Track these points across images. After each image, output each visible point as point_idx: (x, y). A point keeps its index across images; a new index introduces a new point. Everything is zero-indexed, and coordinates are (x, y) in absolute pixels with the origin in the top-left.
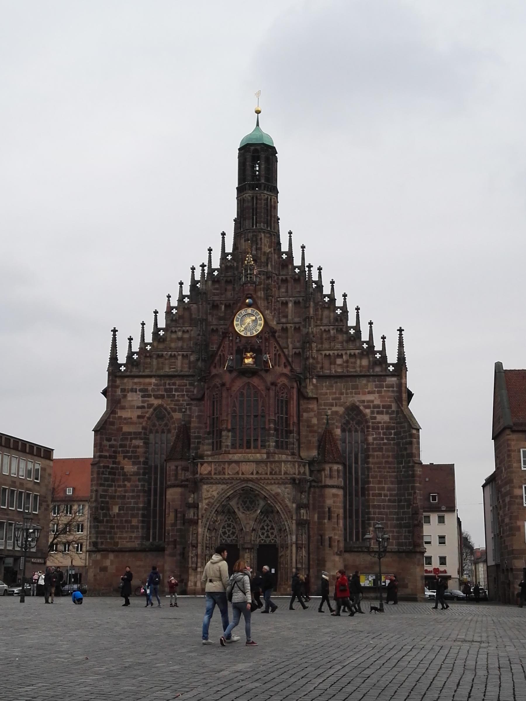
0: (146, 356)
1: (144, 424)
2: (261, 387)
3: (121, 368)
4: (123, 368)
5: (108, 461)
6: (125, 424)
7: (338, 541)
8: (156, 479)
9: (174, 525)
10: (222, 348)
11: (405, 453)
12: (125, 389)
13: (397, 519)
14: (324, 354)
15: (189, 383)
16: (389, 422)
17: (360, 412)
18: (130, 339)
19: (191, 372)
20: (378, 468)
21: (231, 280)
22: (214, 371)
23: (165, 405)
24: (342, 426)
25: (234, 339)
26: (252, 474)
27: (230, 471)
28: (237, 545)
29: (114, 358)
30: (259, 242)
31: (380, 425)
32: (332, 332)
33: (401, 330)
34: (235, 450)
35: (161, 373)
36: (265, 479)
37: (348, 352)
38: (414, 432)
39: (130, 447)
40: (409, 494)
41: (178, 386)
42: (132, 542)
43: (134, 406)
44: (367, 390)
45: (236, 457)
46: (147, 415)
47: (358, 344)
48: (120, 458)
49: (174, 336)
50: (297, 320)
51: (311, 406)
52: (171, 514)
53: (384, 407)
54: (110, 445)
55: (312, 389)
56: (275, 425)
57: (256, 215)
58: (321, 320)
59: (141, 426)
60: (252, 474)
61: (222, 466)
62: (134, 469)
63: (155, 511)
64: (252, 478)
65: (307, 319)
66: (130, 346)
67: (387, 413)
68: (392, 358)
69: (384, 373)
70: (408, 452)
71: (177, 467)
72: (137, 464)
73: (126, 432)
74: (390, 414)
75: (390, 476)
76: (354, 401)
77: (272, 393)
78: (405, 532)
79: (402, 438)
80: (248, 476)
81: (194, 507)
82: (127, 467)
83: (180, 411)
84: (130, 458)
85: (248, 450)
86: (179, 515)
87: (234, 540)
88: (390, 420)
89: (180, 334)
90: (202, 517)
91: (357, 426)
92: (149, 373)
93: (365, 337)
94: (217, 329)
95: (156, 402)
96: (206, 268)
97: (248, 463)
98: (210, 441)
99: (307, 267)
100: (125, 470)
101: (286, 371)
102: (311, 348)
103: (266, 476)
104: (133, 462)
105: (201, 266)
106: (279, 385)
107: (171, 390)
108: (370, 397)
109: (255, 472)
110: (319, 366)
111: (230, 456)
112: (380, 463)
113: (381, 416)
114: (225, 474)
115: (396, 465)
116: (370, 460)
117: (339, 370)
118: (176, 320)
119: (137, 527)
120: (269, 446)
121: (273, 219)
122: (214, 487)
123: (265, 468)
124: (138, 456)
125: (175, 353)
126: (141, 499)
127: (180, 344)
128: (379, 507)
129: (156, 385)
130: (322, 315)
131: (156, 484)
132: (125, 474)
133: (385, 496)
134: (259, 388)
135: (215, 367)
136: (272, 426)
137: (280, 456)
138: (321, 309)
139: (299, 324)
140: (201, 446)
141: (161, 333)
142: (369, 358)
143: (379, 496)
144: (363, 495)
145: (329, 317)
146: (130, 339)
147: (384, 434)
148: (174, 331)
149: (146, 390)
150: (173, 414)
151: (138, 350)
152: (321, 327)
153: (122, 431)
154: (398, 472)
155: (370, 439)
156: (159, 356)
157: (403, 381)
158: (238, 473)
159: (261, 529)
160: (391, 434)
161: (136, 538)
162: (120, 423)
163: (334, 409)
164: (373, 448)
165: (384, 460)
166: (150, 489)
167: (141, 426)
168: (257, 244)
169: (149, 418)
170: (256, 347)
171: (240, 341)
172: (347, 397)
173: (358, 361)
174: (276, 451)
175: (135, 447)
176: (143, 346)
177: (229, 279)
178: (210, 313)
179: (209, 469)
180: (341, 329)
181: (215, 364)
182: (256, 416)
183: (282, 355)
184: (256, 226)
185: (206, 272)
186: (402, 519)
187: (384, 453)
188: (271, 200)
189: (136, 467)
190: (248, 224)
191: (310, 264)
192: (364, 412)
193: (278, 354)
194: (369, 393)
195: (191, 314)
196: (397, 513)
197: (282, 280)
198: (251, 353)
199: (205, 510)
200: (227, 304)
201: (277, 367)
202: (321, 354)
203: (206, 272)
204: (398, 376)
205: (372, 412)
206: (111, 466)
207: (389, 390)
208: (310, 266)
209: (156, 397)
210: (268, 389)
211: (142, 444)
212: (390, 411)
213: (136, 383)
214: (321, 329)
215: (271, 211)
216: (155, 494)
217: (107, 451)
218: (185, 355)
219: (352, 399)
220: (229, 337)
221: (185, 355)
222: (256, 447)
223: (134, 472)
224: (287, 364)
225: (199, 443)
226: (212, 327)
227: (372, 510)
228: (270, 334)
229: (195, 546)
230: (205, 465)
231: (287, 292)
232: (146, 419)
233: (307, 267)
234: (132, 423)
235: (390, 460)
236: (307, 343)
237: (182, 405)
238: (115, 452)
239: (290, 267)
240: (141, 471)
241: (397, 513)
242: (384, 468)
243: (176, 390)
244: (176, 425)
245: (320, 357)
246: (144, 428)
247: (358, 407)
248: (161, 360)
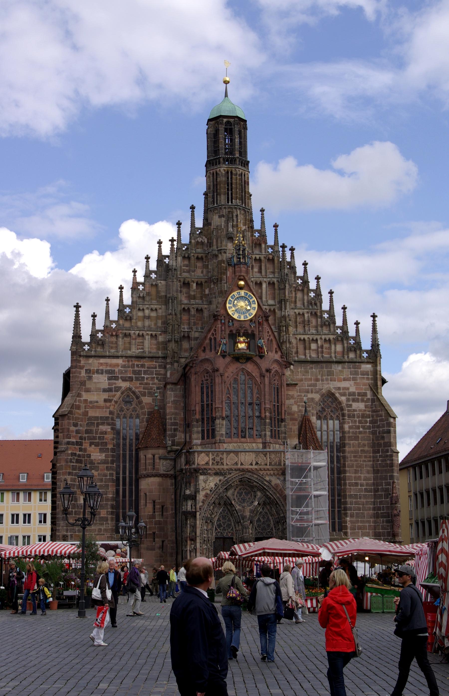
0: (112, 335)
1: (112, 408)
2: (256, 374)
3: (84, 347)
4: (86, 347)
5: (75, 448)
6: (92, 408)
8: (124, 467)
9: (153, 516)
10: (212, 331)
11: (382, 442)
12: (90, 370)
13: (374, 509)
14: (298, 339)
15: (159, 366)
16: (365, 410)
17: (336, 399)
18: (94, 316)
19: (160, 354)
20: (355, 457)
21: (202, 256)
22: (202, 356)
23: (134, 389)
24: (317, 413)
25: (227, 323)
26: (251, 464)
27: (229, 462)
28: (232, 538)
29: (77, 336)
30: (235, 219)
32: (306, 315)
33: (374, 316)
34: (229, 440)
35: (129, 353)
36: (264, 470)
37: (323, 337)
38: (392, 420)
39: (96, 433)
40: (388, 484)
41: (148, 368)
42: (101, 534)
43: (99, 389)
44: (342, 377)
45: (231, 447)
46: (115, 399)
47: (332, 329)
48: (86, 445)
49: (140, 314)
50: (271, 302)
51: (291, 393)
52: (148, 504)
53: (359, 394)
54: (76, 431)
55: (290, 375)
56: (270, 413)
57: (232, 190)
58: (295, 302)
60: (251, 464)
61: (221, 456)
62: (102, 456)
63: (124, 502)
64: (252, 469)
65: (282, 302)
66: (94, 324)
67: (363, 401)
68: (366, 345)
69: (358, 360)
70: (386, 440)
71: (154, 456)
72: (104, 452)
73: (93, 417)
74: (366, 402)
75: (366, 466)
76: (330, 388)
77: (267, 380)
78: (383, 522)
79: (378, 427)
80: (247, 467)
81: (192, 499)
82: (94, 454)
83: (151, 394)
84: (97, 445)
85: (243, 440)
86: (157, 506)
87: (230, 532)
88: (365, 408)
89: (147, 312)
90: (200, 509)
91: (332, 414)
92: (116, 354)
93: (339, 322)
94: (189, 309)
95: (124, 385)
96: (175, 243)
97: (247, 453)
98: (200, 429)
99: (281, 247)
100: (92, 458)
101: (277, 356)
102: (287, 331)
103: (265, 467)
104: (100, 449)
105: (170, 240)
106: (273, 372)
107: (139, 372)
108: (344, 383)
109: (254, 463)
110: (294, 350)
111: (225, 445)
112: (356, 452)
113: (357, 404)
114: (223, 465)
115: (371, 455)
116: (347, 449)
117: (314, 355)
118: (143, 298)
119: (106, 519)
120: (265, 435)
121: (247, 195)
122: (211, 478)
123: (265, 458)
124: (106, 443)
125: (144, 332)
126: (110, 489)
127: (147, 323)
128: (356, 496)
129: (124, 366)
131: (124, 473)
132: (92, 462)
133: (362, 485)
134: (254, 375)
135: (204, 351)
136: (268, 414)
137: (274, 445)
138: (295, 291)
139: (274, 307)
140: (178, 433)
141: (127, 310)
142: (343, 344)
143: (356, 486)
144: (339, 484)
145: (303, 300)
146: (94, 316)
147: (360, 422)
148: (141, 308)
149: (113, 372)
150: (142, 398)
151: (102, 328)
152: (296, 311)
153: (88, 416)
154: (373, 461)
155: (346, 427)
156: (126, 335)
157: (378, 368)
158: (236, 464)
159: (257, 521)
160: (366, 422)
161: (106, 530)
162: (85, 407)
163: (310, 396)
164: (349, 437)
165: (360, 449)
166: (118, 479)
167: (108, 410)
168: (233, 221)
169: (116, 402)
170: (250, 332)
171: (233, 325)
172: (322, 384)
173: (333, 346)
174: (272, 441)
175: (102, 433)
176: (108, 324)
177: (200, 256)
178: (181, 292)
179: (207, 459)
180: (316, 313)
181: (205, 348)
182: (250, 404)
183: (274, 340)
184: (232, 202)
185: (175, 247)
186: (379, 509)
187: (360, 441)
188: (244, 175)
189: (104, 455)
190: (223, 199)
191: (283, 244)
192: (340, 400)
194: (345, 380)
195: (158, 292)
196: (374, 503)
197: (256, 259)
198: (244, 338)
199: (203, 502)
200: (199, 282)
201: (270, 353)
202: (296, 338)
203: (175, 247)
204: (372, 363)
205: (348, 400)
206: (78, 453)
207: (364, 378)
208: (284, 247)
209: (124, 380)
210: (262, 376)
211: (110, 430)
212: (365, 399)
213: (101, 364)
214: (295, 313)
215: (245, 187)
216: (124, 484)
217: (74, 437)
218: (154, 335)
219: (327, 386)
220: (221, 320)
221: (154, 335)
222: (251, 436)
223: (101, 460)
224: (277, 350)
225: (175, 430)
226: (183, 306)
227: (348, 500)
228: (264, 319)
229: (193, 540)
230: (203, 454)
231: (260, 271)
232: (113, 403)
233: (281, 247)
234: (99, 407)
235: (366, 448)
236: (283, 326)
237: (151, 388)
238: (81, 438)
239: (263, 246)
240: (110, 459)
241: (374, 503)
242: (360, 457)
243: (145, 372)
244: (146, 410)
245: (294, 341)
246: (111, 413)
247: (333, 394)
248: (127, 340)
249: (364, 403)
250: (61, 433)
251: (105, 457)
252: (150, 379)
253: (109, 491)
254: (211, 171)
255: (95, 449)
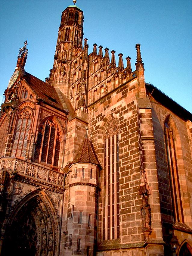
7: (79, 240)
31: (126, 122)
32: (99, 75)
33: (138, 46)
37: (106, 81)
53: (128, 106)
67: (131, 109)
112: (127, 155)
130: (94, 68)
133: (132, 185)
147: (130, 127)
152: (93, 75)
163: (97, 124)
164: (121, 144)
165: (129, 151)
187: (130, 144)
188: (69, 28)
193: (25, 90)
205: (121, 115)
212: (133, 107)
242: (130, 158)
249: (132, 111)
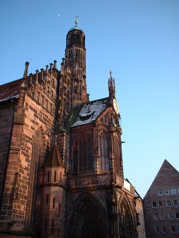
59: (32, 134)
73: (25, 135)
82: (23, 161)
84: (25, 155)
100: (22, 163)
150: (45, 135)
234: (28, 130)
250: (15, 136)
251: (28, 166)
252: (49, 126)
253: (27, 191)
254: (69, 50)
255: (24, 157)
